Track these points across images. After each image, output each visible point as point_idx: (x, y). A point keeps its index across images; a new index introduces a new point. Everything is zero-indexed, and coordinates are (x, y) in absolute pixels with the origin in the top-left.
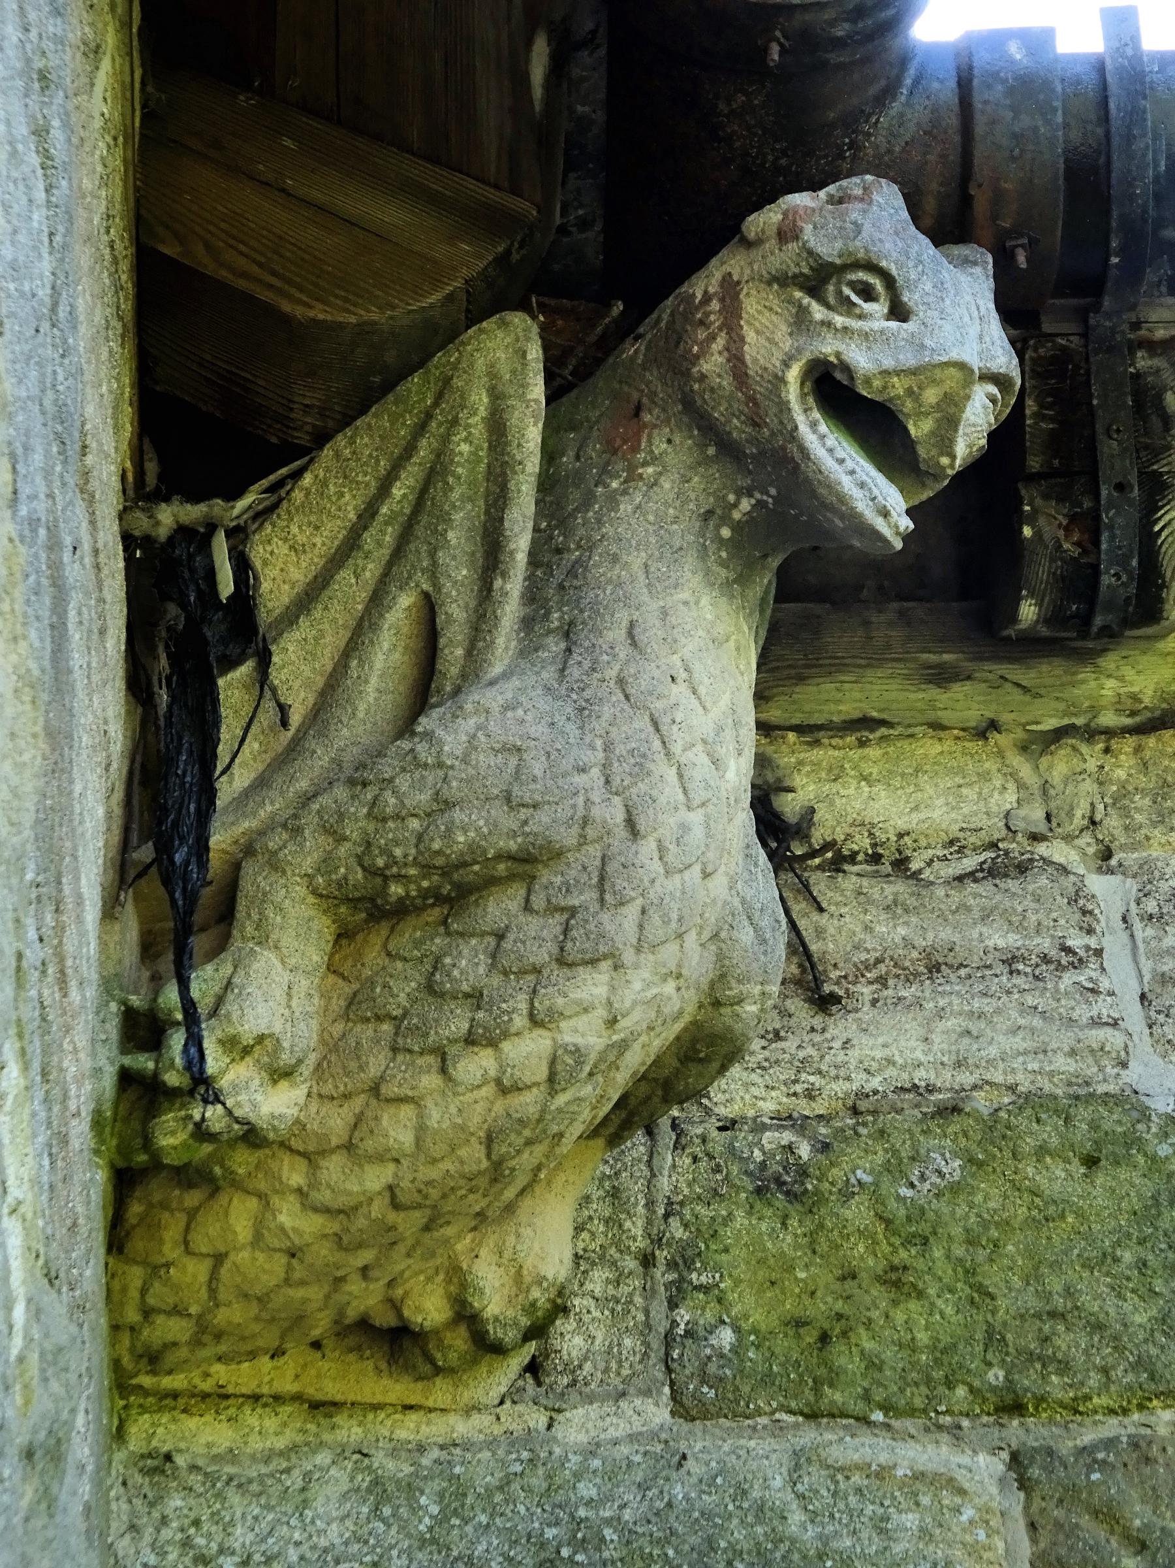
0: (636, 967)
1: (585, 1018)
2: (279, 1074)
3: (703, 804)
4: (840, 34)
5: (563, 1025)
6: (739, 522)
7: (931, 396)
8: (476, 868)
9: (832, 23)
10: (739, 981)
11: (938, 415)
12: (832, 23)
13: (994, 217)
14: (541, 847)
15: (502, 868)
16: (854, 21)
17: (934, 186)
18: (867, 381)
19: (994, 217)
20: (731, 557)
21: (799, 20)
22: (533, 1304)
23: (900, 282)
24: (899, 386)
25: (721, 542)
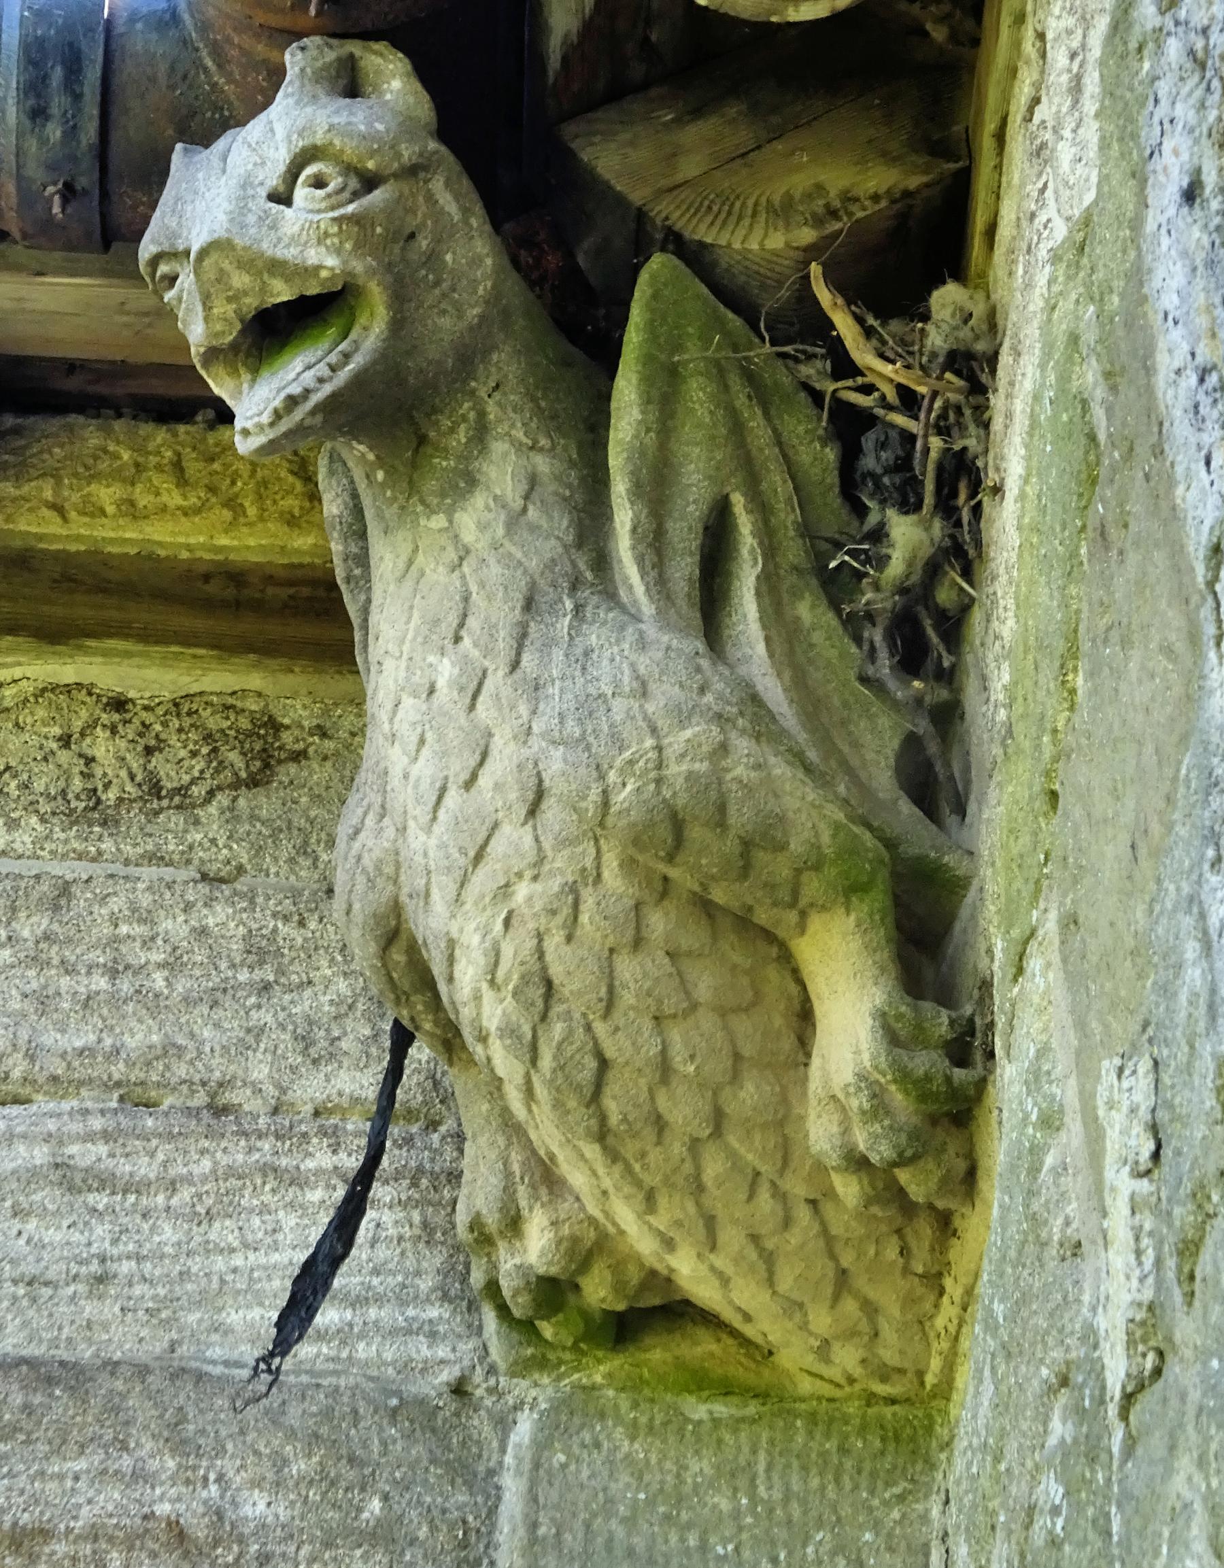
0: (461, 930)
1: (485, 1000)
2: (514, 1224)
3: (422, 741)
4: (58, 133)
5: (485, 1023)
6: (377, 457)
7: (240, 280)
8: (395, 975)
9: (43, 141)
10: (584, 798)
11: (266, 276)
12: (43, 141)
13: (282, 11)
14: (377, 924)
15: (398, 956)
16: (47, 118)
17: (260, 47)
18: (217, 335)
19: (282, 11)
20: (393, 488)
21: (34, 171)
22: (864, 1113)
23: (166, 247)
24: (222, 308)
25: (383, 486)
